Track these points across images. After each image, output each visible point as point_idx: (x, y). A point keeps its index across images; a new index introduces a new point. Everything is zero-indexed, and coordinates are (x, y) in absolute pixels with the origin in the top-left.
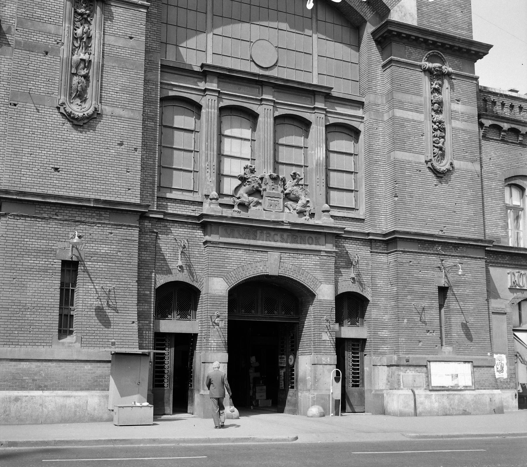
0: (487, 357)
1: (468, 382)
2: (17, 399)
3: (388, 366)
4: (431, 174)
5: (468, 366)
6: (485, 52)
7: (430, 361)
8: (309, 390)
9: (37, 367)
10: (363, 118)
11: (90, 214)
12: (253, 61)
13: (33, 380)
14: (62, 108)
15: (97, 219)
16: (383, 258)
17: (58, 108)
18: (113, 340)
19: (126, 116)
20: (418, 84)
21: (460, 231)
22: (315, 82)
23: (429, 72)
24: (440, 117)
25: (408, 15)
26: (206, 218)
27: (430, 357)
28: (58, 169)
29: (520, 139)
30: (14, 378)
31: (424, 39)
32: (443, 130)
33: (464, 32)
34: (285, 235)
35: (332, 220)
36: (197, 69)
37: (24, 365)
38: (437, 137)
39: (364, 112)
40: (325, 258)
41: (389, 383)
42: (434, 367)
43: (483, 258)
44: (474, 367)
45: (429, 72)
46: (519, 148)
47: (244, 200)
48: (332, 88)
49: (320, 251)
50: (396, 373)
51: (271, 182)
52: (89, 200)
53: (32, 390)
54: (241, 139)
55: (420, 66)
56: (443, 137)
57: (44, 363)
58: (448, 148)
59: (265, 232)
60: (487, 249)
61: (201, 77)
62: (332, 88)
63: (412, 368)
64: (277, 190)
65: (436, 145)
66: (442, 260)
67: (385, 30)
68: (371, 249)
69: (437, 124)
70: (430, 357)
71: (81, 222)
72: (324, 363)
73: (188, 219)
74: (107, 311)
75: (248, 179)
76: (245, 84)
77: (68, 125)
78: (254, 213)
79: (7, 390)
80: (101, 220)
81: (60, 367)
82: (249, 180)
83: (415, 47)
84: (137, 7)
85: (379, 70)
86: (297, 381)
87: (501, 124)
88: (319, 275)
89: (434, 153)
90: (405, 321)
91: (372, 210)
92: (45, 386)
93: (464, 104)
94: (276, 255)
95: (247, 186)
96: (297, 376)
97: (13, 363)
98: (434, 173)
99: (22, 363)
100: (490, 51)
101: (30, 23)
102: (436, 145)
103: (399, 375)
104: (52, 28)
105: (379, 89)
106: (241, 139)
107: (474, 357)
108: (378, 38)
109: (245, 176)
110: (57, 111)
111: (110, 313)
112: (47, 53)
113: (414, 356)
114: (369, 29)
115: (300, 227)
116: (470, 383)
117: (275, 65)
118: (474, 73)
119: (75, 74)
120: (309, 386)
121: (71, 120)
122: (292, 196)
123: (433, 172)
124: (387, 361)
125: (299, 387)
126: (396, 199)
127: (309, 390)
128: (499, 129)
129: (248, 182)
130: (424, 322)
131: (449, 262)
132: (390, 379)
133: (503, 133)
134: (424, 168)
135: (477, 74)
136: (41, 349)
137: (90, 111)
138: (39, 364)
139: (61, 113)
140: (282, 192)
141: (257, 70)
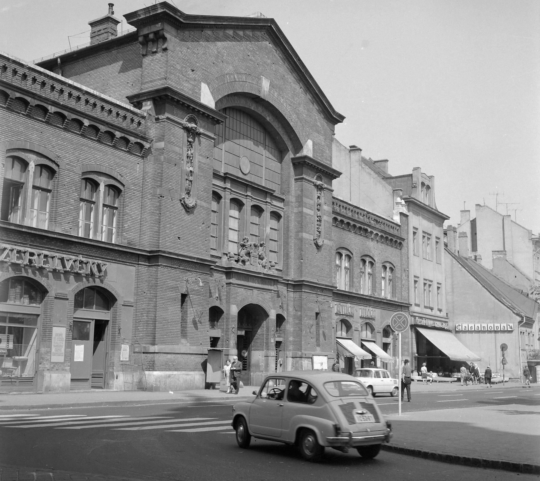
0: (332, 353)
1: (325, 367)
2: (169, 376)
3: (292, 357)
4: (315, 246)
5: (326, 358)
7: (313, 355)
8: (263, 371)
9: (174, 357)
10: (283, 209)
11: (192, 266)
12: (240, 169)
13: (173, 365)
14: (183, 200)
15: (195, 269)
16: (291, 295)
17: (181, 200)
18: (201, 342)
19: (206, 207)
21: (323, 280)
22: (263, 185)
23: (317, 186)
24: (319, 213)
25: (309, 151)
26: (233, 269)
27: (313, 353)
28: (179, 237)
29: (343, 226)
30: (166, 364)
31: (326, 171)
32: (320, 221)
33: (329, 162)
34: (259, 280)
35: (276, 272)
36: (222, 175)
37: (169, 356)
39: (284, 206)
40: (273, 294)
41: (294, 368)
42: (315, 358)
43: (331, 297)
44: (328, 358)
45: (317, 186)
46: (342, 230)
47: (245, 258)
48: (275, 191)
49: (272, 290)
50: (300, 362)
51: (253, 247)
52: (194, 258)
53: (173, 371)
54: (234, 218)
55: (313, 183)
57: (177, 355)
58: (322, 233)
59: (252, 278)
60: (334, 291)
61: (222, 179)
62: (275, 191)
63: (306, 359)
64: (256, 253)
66: (317, 297)
67: (303, 160)
68: (287, 289)
70: (313, 353)
71: (189, 271)
72: (272, 356)
73: (221, 269)
74: (198, 324)
76: (240, 185)
77: (184, 211)
79: (164, 371)
80: (196, 269)
81: (182, 357)
82: (247, 246)
83: (311, 170)
84: (211, 139)
85: (293, 181)
86: (249, 366)
88: (271, 304)
90: (304, 331)
91: (287, 265)
92: (178, 369)
93: (328, 206)
94: (255, 291)
95: (245, 250)
96: (249, 363)
97: (165, 355)
98: (316, 247)
99: (168, 355)
101: (169, 145)
102: (318, 230)
103: (302, 363)
104: (177, 149)
105: (293, 192)
106: (234, 218)
107: (328, 353)
108: (296, 162)
109: (245, 244)
110: (179, 202)
111: (199, 324)
112: (176, 165)
113: (308, 352)
114: (290, 155)
115: (267, 276)
116: (327, 368)
117: (249, 173)
118: (331, 186)
120: (261, 369)
121: (186, 208)
123: (316, 245)
124: (292, 354)
125: (252, 369)
126: (302, 261)
127: (263, 371)
129: (246, 247)
130: (310, 333)
131: (321, 298)
132: (294, 365)
133: (337, 222)
134: (313, 242)
135: (333, 188)
136: (176, 347)
138: (174, 355)
139: (182, 204)
140: (258, 254)
141: (240, 175)
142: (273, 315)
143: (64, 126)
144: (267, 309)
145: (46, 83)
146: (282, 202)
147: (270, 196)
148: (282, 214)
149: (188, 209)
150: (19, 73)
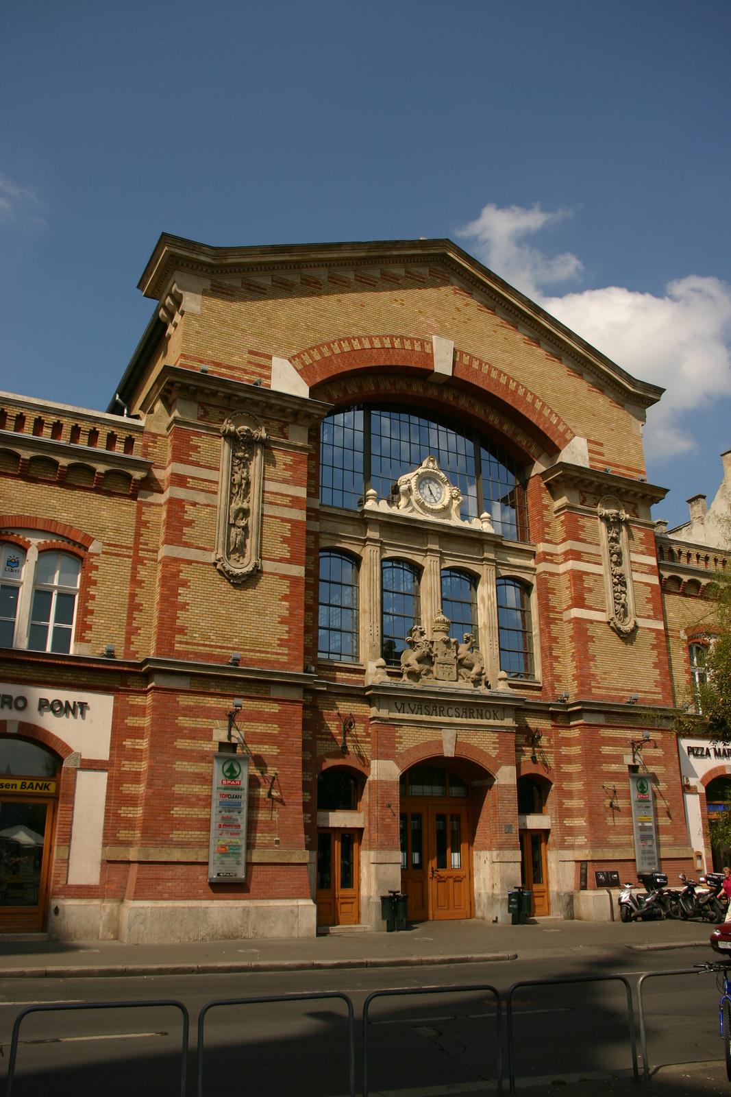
6: (662, 496)
20: (596, 532)
23: (605, 519)
24: (618, 570)
32: (624, 584)
38: (617, 592)
56: (624, 593)
58: (631, 607)
65: (618, 601)
69: (618, 577)
75: (417, 643)
78: (426, 683)
87: (682, 576)
89: (616, 611)
100: (667, 495)
102: (618, 601)
119: (234, 525)
122: (465, 661)
128: (679, 580)
129: (419, 646)
137: (250, 568)
140: (456, 658)
142: (506, 776)
143: (94, 485)
144: (488, 766)
145: (62, 424)
146: (530, 559)
147: (493, 549)
148: (534, 582)
149: (628, 637)
150: (47, 422)
